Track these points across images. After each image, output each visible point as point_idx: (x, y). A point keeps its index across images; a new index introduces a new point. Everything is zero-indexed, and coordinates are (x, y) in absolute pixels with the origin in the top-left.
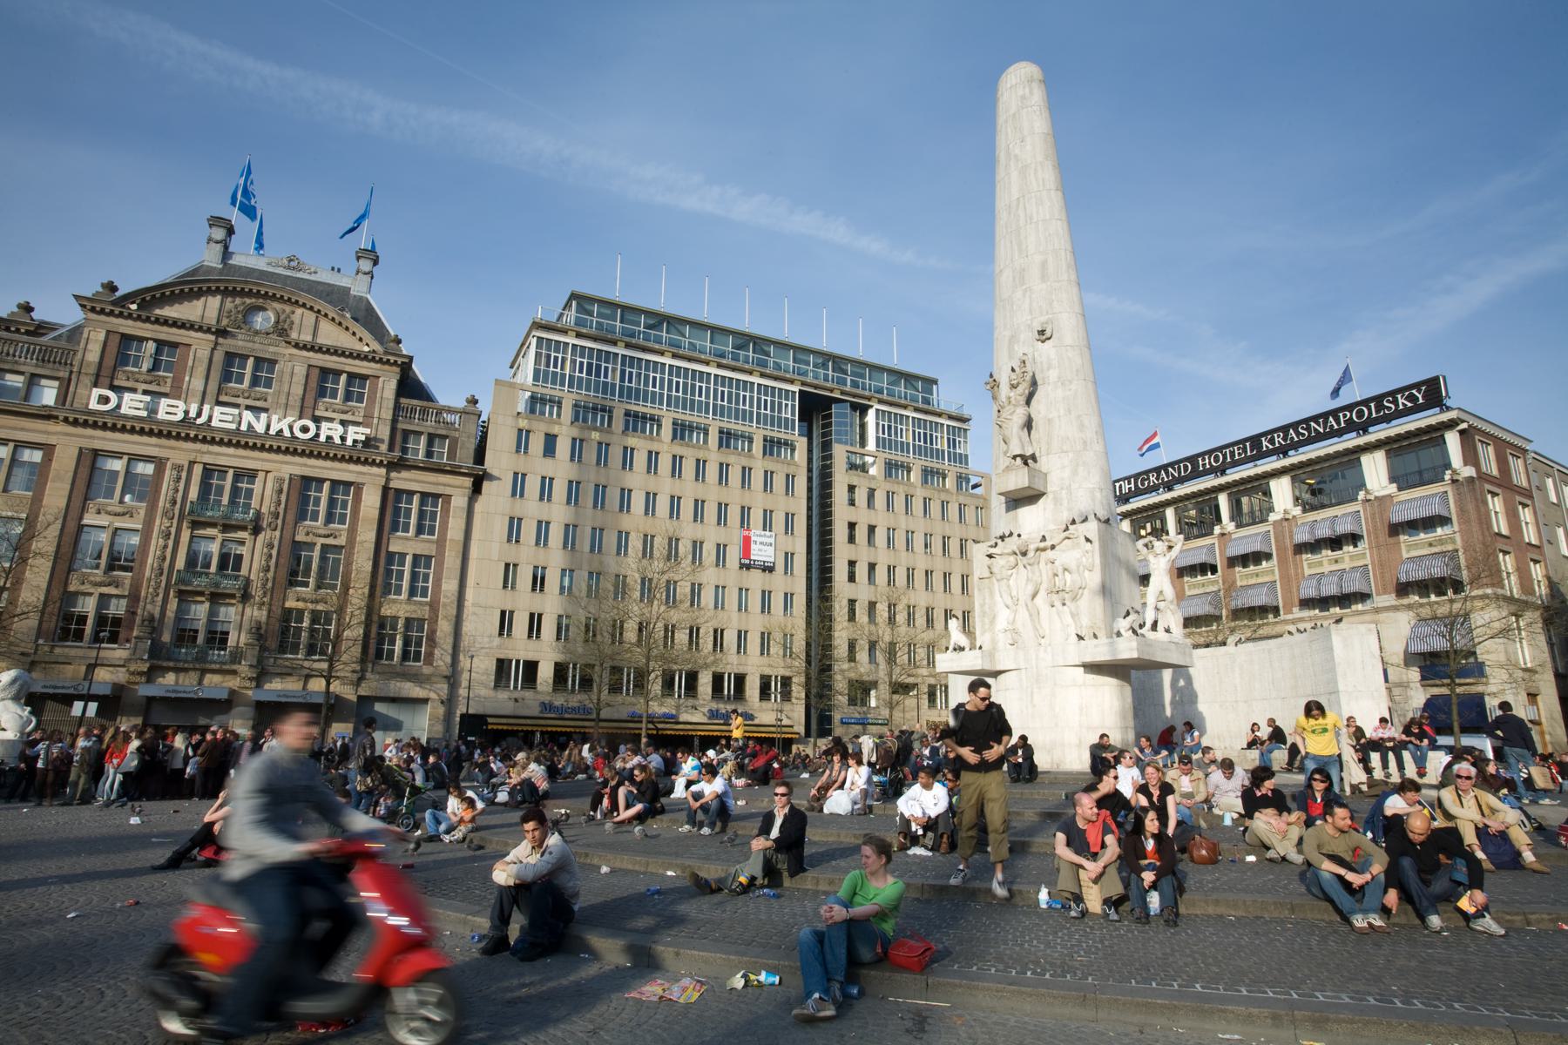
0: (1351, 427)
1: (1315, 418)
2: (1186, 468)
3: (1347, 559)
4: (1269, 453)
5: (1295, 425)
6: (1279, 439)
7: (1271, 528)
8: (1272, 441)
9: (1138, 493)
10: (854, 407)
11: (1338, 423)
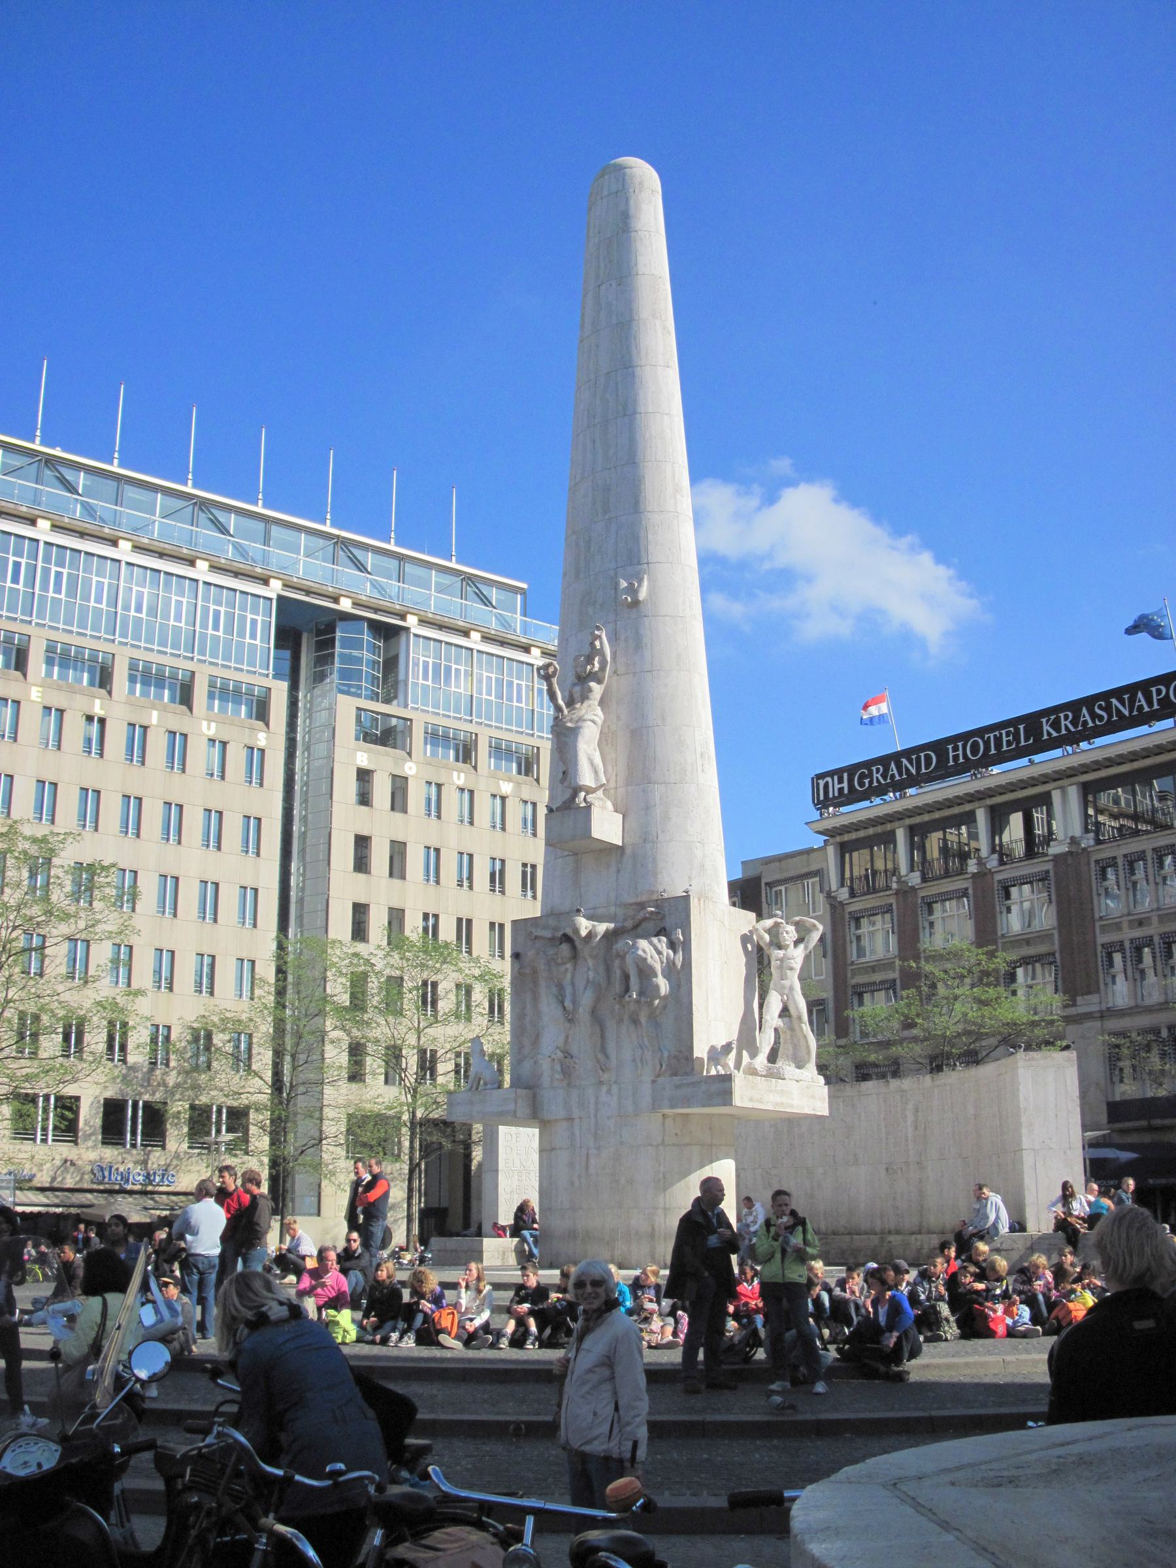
1: (1117, 693)
2: (928, 759)
3: (1155, 920)
5: (1089, 702)
7: (1049, 866)
8: (1056, 725)
9: (853, 797)
10: (378, 629)
11: (1150, 704)
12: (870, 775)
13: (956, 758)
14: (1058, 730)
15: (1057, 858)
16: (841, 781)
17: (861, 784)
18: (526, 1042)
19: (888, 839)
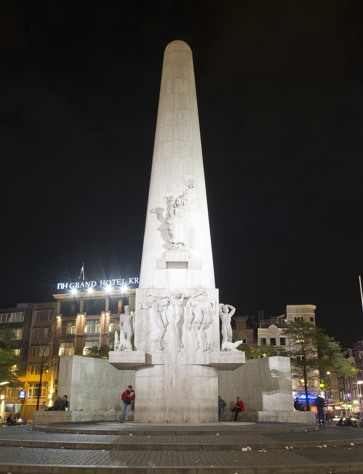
14: (134, 282)
18: (143, 334)
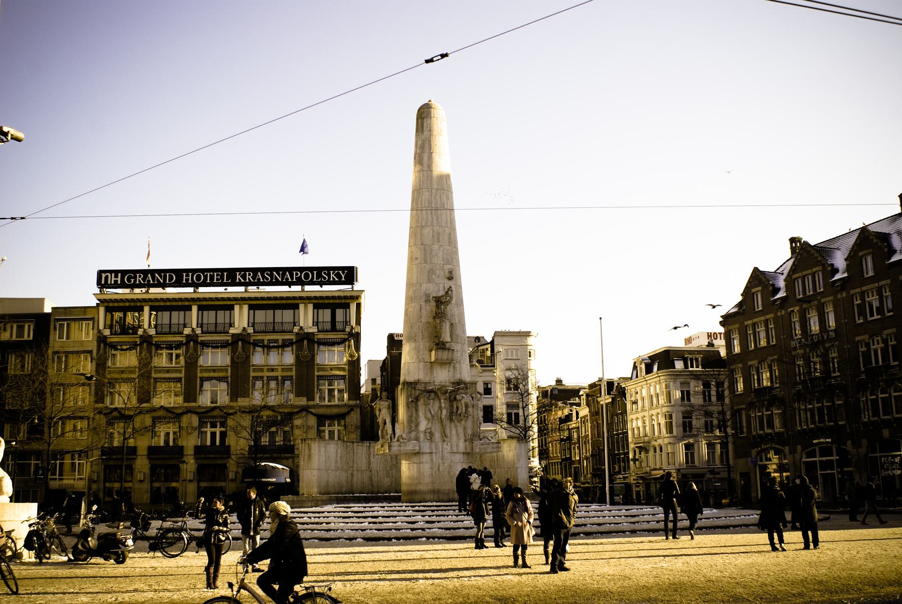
0: (299, 282)
1: (277, 270)
2: (171, 278)
3: (280, 370)
4: (240, 284)
5: (263, 270)
6: (249, 277)
7: (230, 338)
8: (244, 277)
9: (123, 285)
11: (292, 278)
12: (135, 278)
13: (187, 280)
14: (245, 279)
15: (233, 335)
16: (116, 276)
17: (129, 280)
18: (413, 425)
19: (140, 310)
